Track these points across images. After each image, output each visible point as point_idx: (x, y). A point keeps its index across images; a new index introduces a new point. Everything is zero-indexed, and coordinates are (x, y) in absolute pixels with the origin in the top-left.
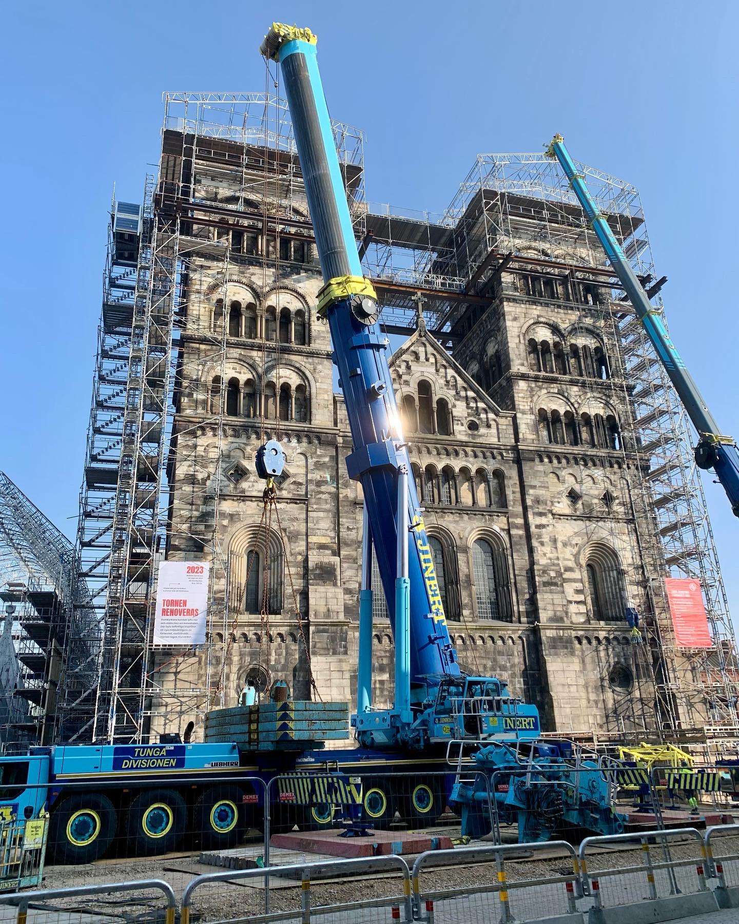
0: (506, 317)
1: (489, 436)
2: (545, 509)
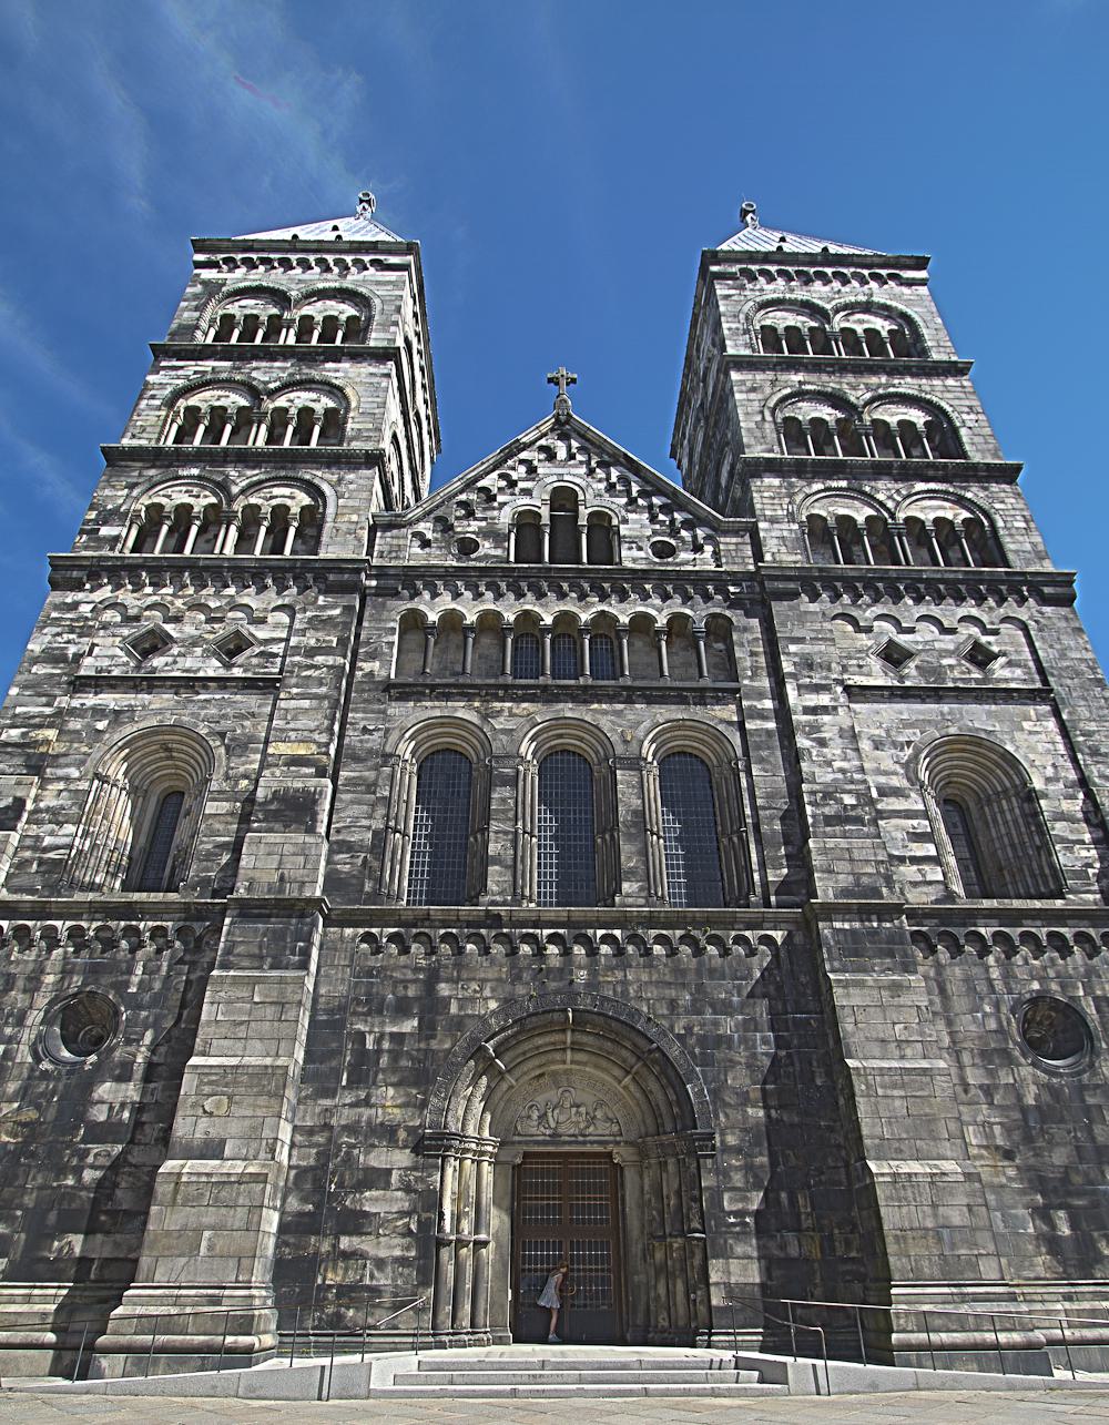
2: (827, 678)
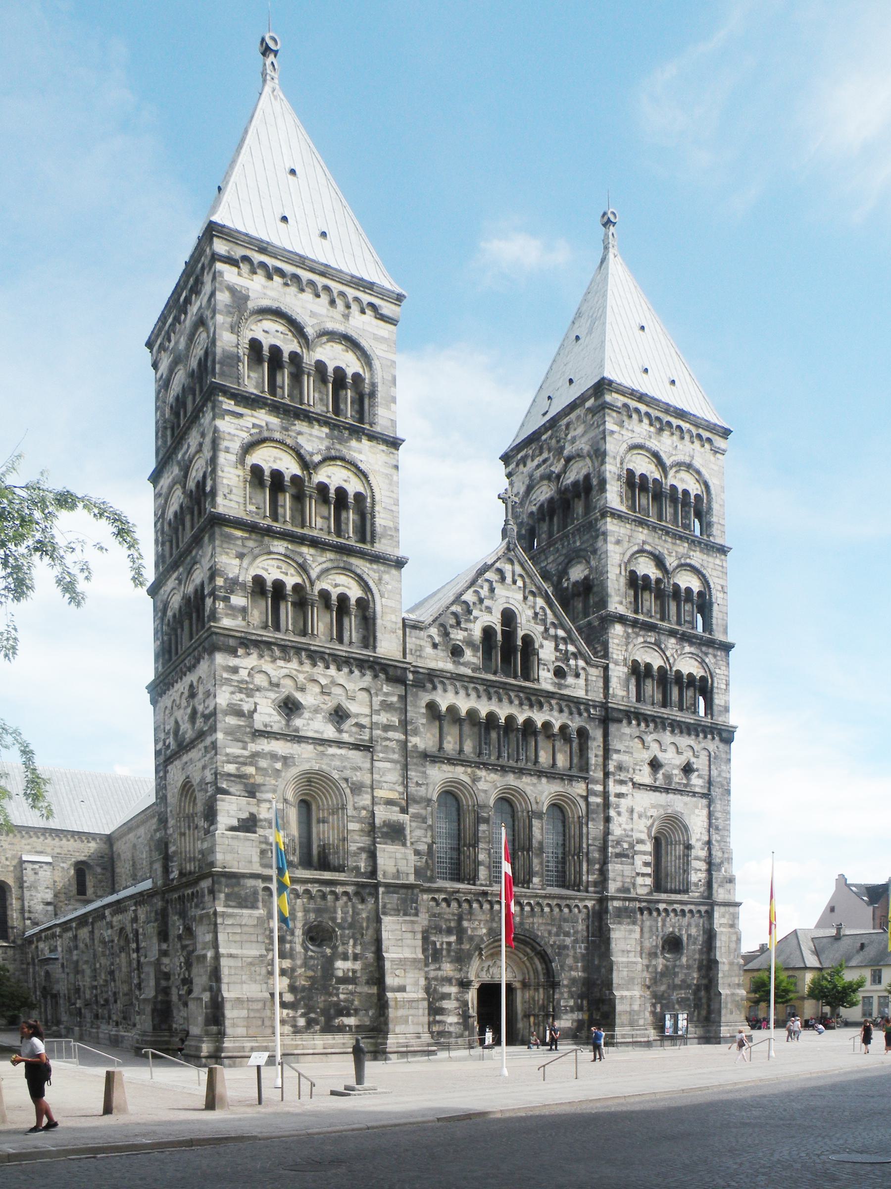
0: (609, 538)
1: (576, 688)
2: (626, 777)
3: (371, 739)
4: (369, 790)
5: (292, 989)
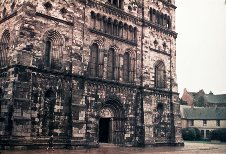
1: (135, 13)
3: (73, 22)
4: (71, 40)
5: (39, 116)
